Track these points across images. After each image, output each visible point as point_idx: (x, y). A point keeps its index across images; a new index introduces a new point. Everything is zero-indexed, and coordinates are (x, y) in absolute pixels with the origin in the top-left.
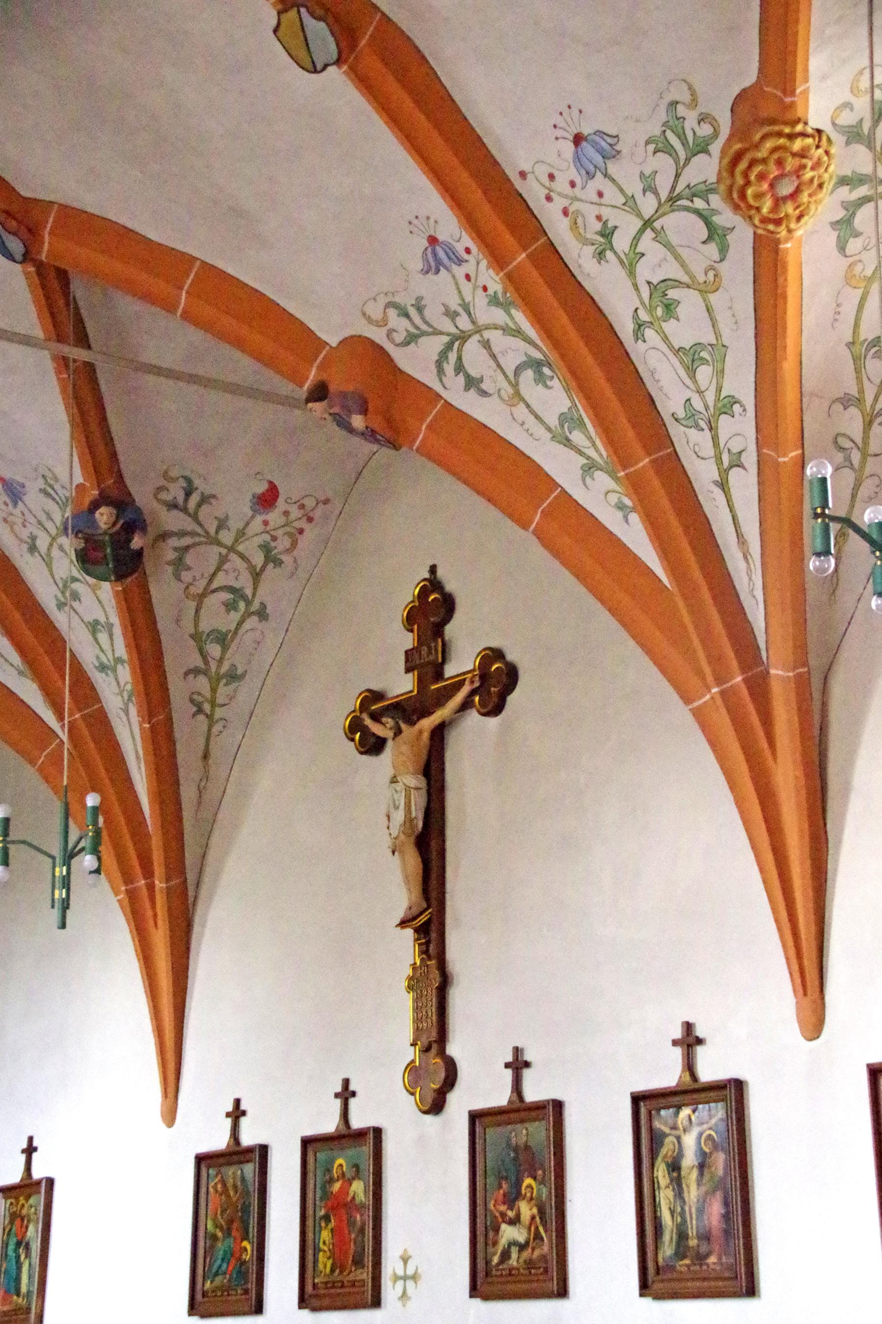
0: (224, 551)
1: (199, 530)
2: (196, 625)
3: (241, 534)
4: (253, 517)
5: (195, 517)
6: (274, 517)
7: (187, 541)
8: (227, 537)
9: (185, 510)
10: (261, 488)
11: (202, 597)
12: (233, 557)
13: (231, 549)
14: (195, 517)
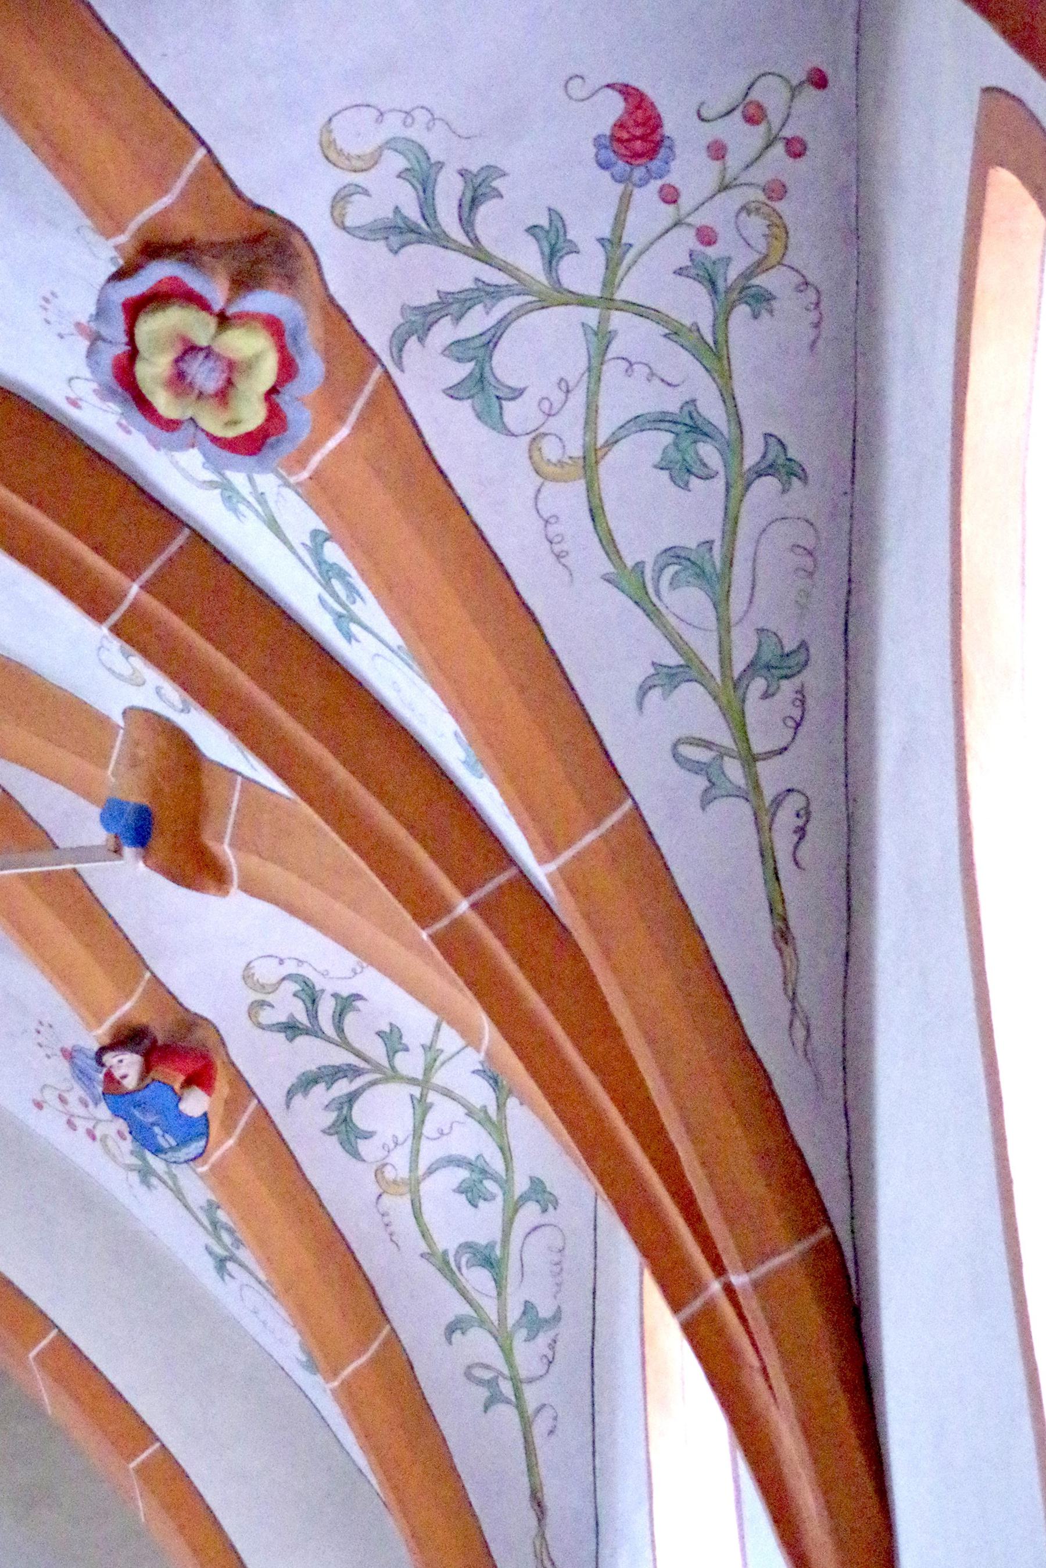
0: (591, 316)
1: (499, 278)
2: (609, 545)
3: (614, 246)
4: (625, 202)
5: (478, 252)
6: (688, 168)
7: (477, 321)
8: (583, 273)
9: (441, 240)
10: (614, 107)
11: (589, 463)
12: (618, 319)
13: (607, 302)
14: (478, 252)
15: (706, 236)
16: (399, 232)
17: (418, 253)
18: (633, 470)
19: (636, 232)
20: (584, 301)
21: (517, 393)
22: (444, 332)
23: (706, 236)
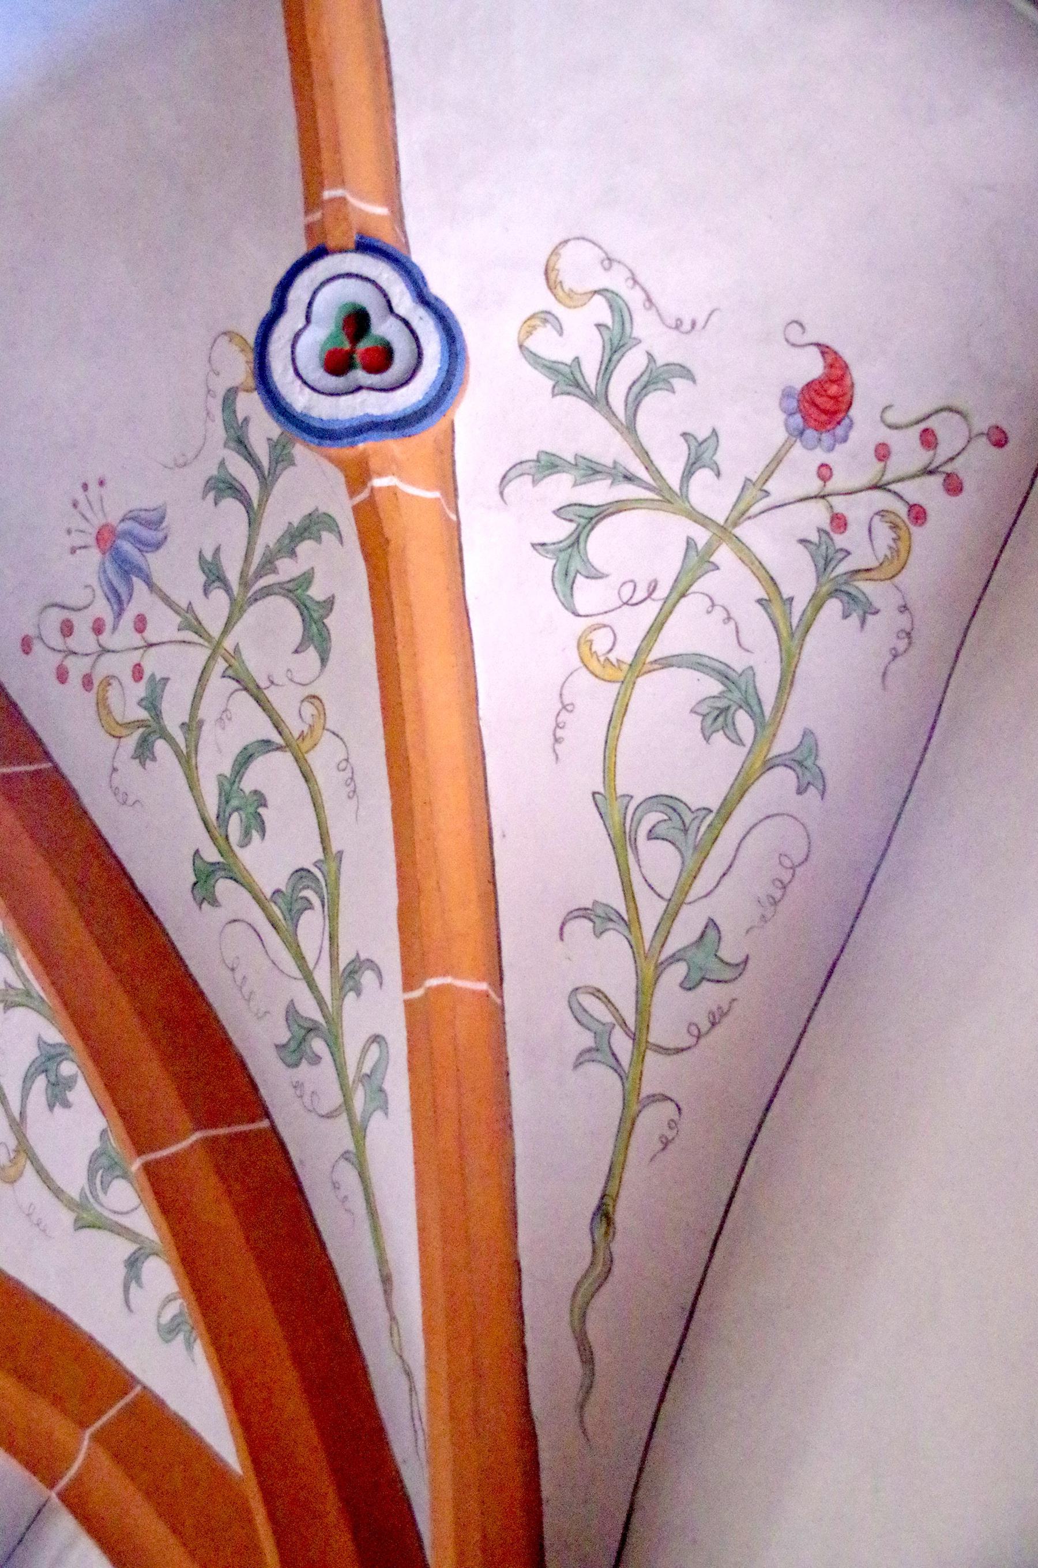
3: (755, 487)
5: (629, 429)
7: (598, 493)
13: (725, 532)
14: (629, 429)
15: (839, 522)
16: (567, 379)
17: (575, 406)
18: (668, 701)
19: (779, 487)
20: (703, 520)
21: (596, 575)
22: (561, 488)
23: (839, 522)
